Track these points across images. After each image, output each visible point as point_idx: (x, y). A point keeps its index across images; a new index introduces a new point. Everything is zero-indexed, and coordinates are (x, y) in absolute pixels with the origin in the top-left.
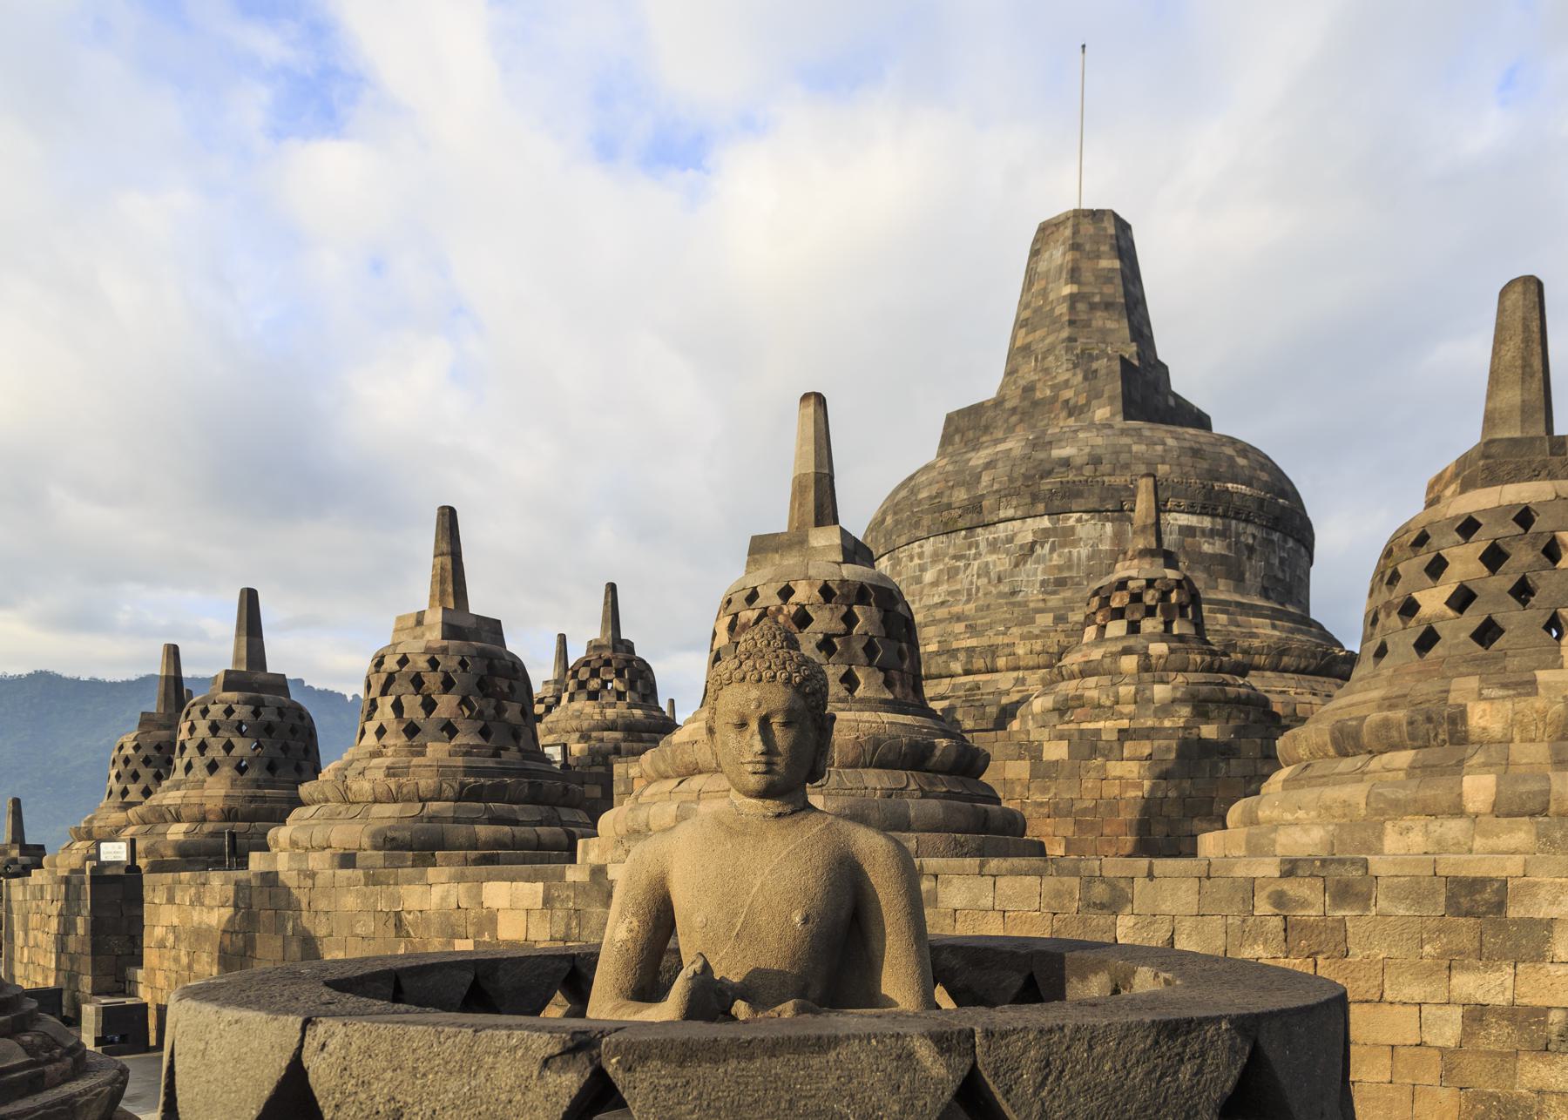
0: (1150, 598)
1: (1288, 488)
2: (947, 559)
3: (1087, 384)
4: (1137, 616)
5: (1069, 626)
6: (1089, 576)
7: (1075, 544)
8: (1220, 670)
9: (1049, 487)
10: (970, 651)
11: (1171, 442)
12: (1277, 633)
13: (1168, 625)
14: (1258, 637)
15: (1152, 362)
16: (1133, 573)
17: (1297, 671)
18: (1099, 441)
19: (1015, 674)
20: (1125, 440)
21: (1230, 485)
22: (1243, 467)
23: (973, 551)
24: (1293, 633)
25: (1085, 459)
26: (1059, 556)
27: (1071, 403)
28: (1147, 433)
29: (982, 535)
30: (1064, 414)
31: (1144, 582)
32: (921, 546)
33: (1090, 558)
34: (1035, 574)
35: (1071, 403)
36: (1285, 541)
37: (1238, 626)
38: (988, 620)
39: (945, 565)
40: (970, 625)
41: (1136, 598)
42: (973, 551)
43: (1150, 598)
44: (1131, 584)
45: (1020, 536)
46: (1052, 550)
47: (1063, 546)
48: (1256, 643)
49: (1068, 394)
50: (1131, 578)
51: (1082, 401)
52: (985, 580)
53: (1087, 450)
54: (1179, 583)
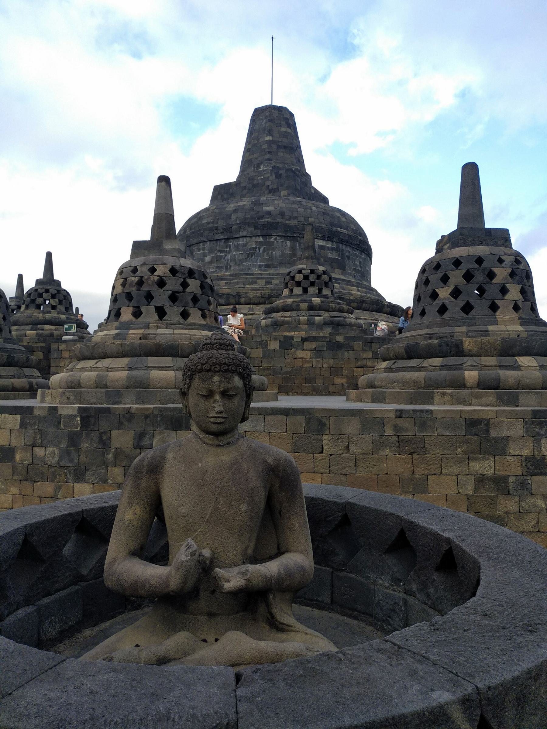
0: (312, 278)
1: (362, 232)
3: (277, 180)
4: (306, 286)
5: (272, 286)
7: (273, 250)
8: (342, 311)
9: (262, 223)
10: (228, 294)
11: (314, 208)
12: (359, 293)
13: (320, 290)
16: (304, 266)
17: (368, 310)
18: (284, 205)
19: (249, 306)
20: (297, 206)
21: (339, 229)
22: (343, 222)
23: (228, 249)
24: (366, 294)
26: (268, 254)
27: (270, 187)
28: (304, 204)
29: (232, 243)
30: (267, 192)
31: (309, 271)
32: (204, 245)
35: (270, 187)
36: (361, 254)
37: (344, 289)
38: (236, 281)
39: (216, 254)
40: (228, 283)
41: (306, 277)
43: (312, 278)
44: (303, 272)
46: (264, 251)
47: (269, 250)
49: (268, 183)
50: (304, 269)
51: (275, 187)
53: (279, 209)
54: (324, 272)
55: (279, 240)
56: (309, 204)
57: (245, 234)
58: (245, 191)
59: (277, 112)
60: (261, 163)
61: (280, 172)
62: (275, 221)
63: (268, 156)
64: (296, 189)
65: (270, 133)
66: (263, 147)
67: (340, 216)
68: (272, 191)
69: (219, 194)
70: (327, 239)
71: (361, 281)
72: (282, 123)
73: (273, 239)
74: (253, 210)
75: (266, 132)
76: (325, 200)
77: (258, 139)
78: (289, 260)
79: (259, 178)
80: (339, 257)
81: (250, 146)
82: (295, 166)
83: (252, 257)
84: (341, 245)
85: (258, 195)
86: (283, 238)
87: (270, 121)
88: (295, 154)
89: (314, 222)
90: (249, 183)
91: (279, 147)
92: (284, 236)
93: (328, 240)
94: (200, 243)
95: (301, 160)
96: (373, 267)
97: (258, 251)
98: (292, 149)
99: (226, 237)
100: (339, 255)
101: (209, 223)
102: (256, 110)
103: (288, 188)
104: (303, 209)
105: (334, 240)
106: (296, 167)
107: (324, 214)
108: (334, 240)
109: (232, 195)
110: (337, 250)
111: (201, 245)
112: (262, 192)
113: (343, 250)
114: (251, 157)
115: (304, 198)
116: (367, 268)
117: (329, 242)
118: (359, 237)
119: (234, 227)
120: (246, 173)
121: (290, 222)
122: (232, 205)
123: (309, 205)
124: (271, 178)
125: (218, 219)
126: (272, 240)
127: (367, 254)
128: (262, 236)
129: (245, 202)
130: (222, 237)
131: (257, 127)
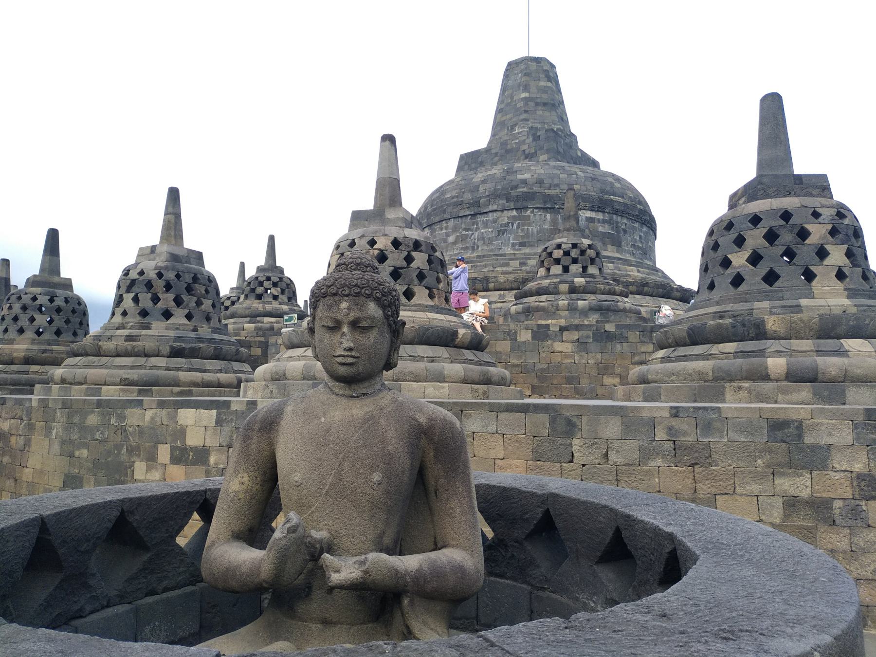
1: (641, 199)
2: (461, 230)
3: (535, 143)
5: (528, 268)
6: (539, 241)
7: (530, 225)
9: (516, 194)
11: (580, 173)
14: (631, 277)
15: (569, 133)
18: (542, 171)
19: (499, 292)
20: (557, 172)
21: (612, 197)
22: (618, 188)
23: (475, 226)
25: (535, 181)
26: (522, 230)
27: (527, 152)
28: (567, 168)
29: (480, 219)
30: (523, 157)
32: (447, 223)
33: (538, 232)
34: (509, 240)
35: (527, 152)
36: (642, 227)
38: (484, 263)
40: (474, 266)
42: (475, 226)
45: (500, 219)
46: (518, 227)
47: (524, 225)
48: (630, 280)
49: (525, 147)
52: (482, 242)
53: (536, 176)
55: (536, 212)
56: (575, 168)
57: (495, 207)
58: (497, 159)
59: (535, 64)
60: (516, 125)
61: (538, 134)
62: (533, 191)
63: (524, 116)
64: (558, 153)
65: (526, 88)
66: (518, 105)
67: (613, 181)
68: (529, 156)
69: (466, 163)
70: (596, 210)
71: (641, 259)
72: (541, 76)
73: (529, 211)
74: (505, 179)
75: (521, 88)
76: (595, 164)
77: (512, 97)
78: (550, 236)
79: (513, 142)
80: (613, 230)
81: (503, 106)
82: (557, 125)
83: (503, 234)
84: (615, 217)
85: (512, 161)
86: (542, 210)
87: (525, 75)
88: (556, 112)
89: (580, 190)
90: (502, 149)
91: (537, 104)
92: (543, 208)
93: (598, 211)
94: (442, 221)
95: (565, 118)
96: (657, 243)
97: (511, 227)
98: (553, 105)
99: (473, 213)
100: (612, 229)
101: (453, 198)
102: (510, 64)
103: (548, 151)
104: (566, 176)
105: (606, 211)
106: (558, 127)
107: (593, 179)
108: (606, 211)
109: (482, 164)
110: (610, 222)
111: (444, 224)
112: (517, 158)
113: (617, 223)
114: (504, 118)
115: (568, 163)
116: (650, 244)
117: (600, 213)
118: (639, 206)
119: (482, 201)
120: (497, 137)
121: (550, 191)
122: (480, 175)
123: (574, 169)
124: (528, 141)
125: (464, 192)
126: (528, 213)
127: (649, 227)
128: (516, 209)
129: (496, 171)
130: (468, 213)
131: (510, 83)
